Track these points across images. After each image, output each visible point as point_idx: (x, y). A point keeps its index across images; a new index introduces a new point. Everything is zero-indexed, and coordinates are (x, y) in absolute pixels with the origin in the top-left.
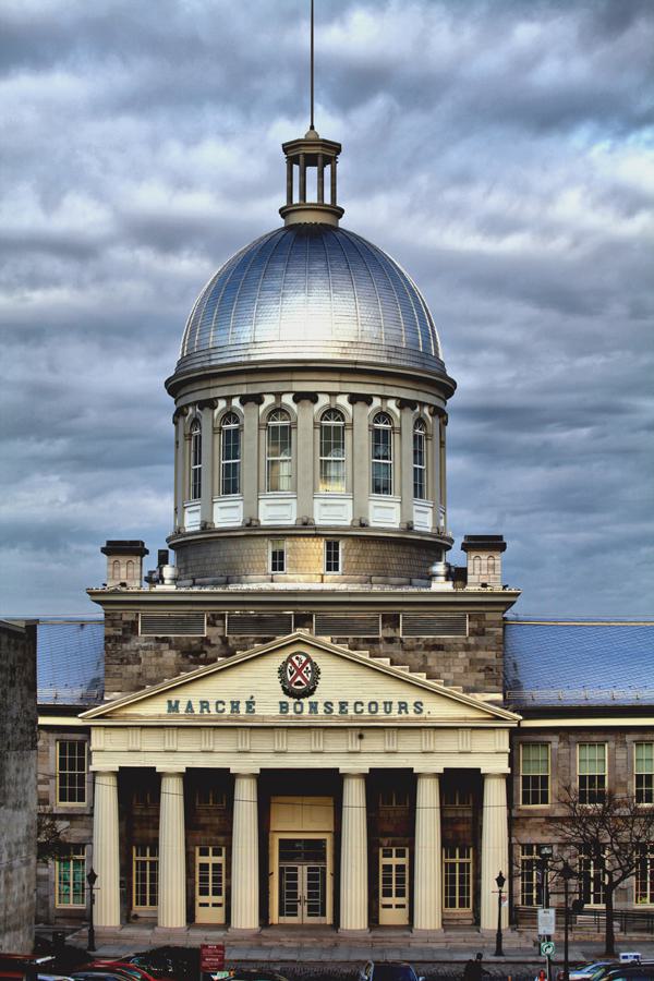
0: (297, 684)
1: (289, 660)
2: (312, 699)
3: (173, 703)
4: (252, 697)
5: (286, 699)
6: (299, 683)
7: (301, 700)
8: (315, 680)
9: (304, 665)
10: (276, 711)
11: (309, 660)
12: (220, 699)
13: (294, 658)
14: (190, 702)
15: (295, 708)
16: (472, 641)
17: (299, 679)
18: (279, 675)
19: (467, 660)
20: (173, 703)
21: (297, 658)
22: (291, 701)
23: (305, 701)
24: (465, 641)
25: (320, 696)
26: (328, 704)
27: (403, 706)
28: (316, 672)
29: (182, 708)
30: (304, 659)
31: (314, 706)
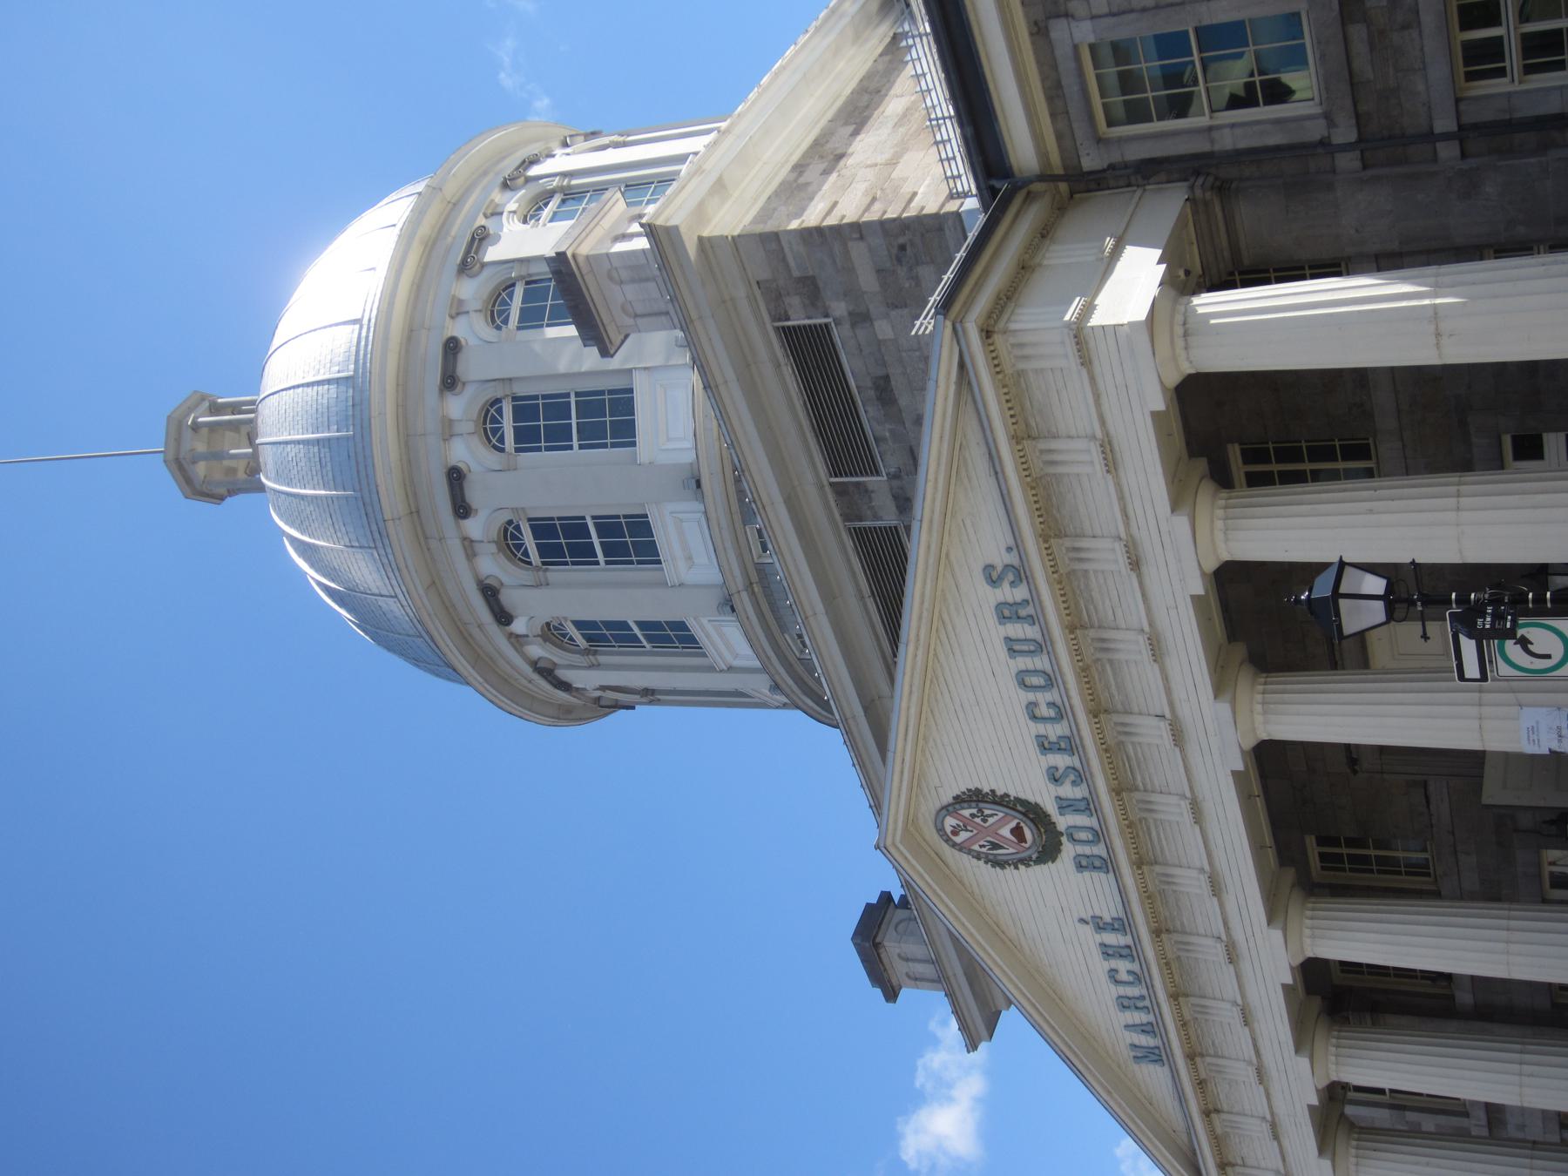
1: (960, 847)
2: (1051, 808)
4: (1082, 921)
6: (1017, 832)
8: (1002, 801)
11: (948, 809)
14: (1127, 1027)
16: (840, 308)
17: (1006, 832)
19: (893, 313)
22: (1068, 850)
23: (1062, 822)
24: (847, 326)
25: (1044, 796)
28: (975, 797)
31: (1065, 805)
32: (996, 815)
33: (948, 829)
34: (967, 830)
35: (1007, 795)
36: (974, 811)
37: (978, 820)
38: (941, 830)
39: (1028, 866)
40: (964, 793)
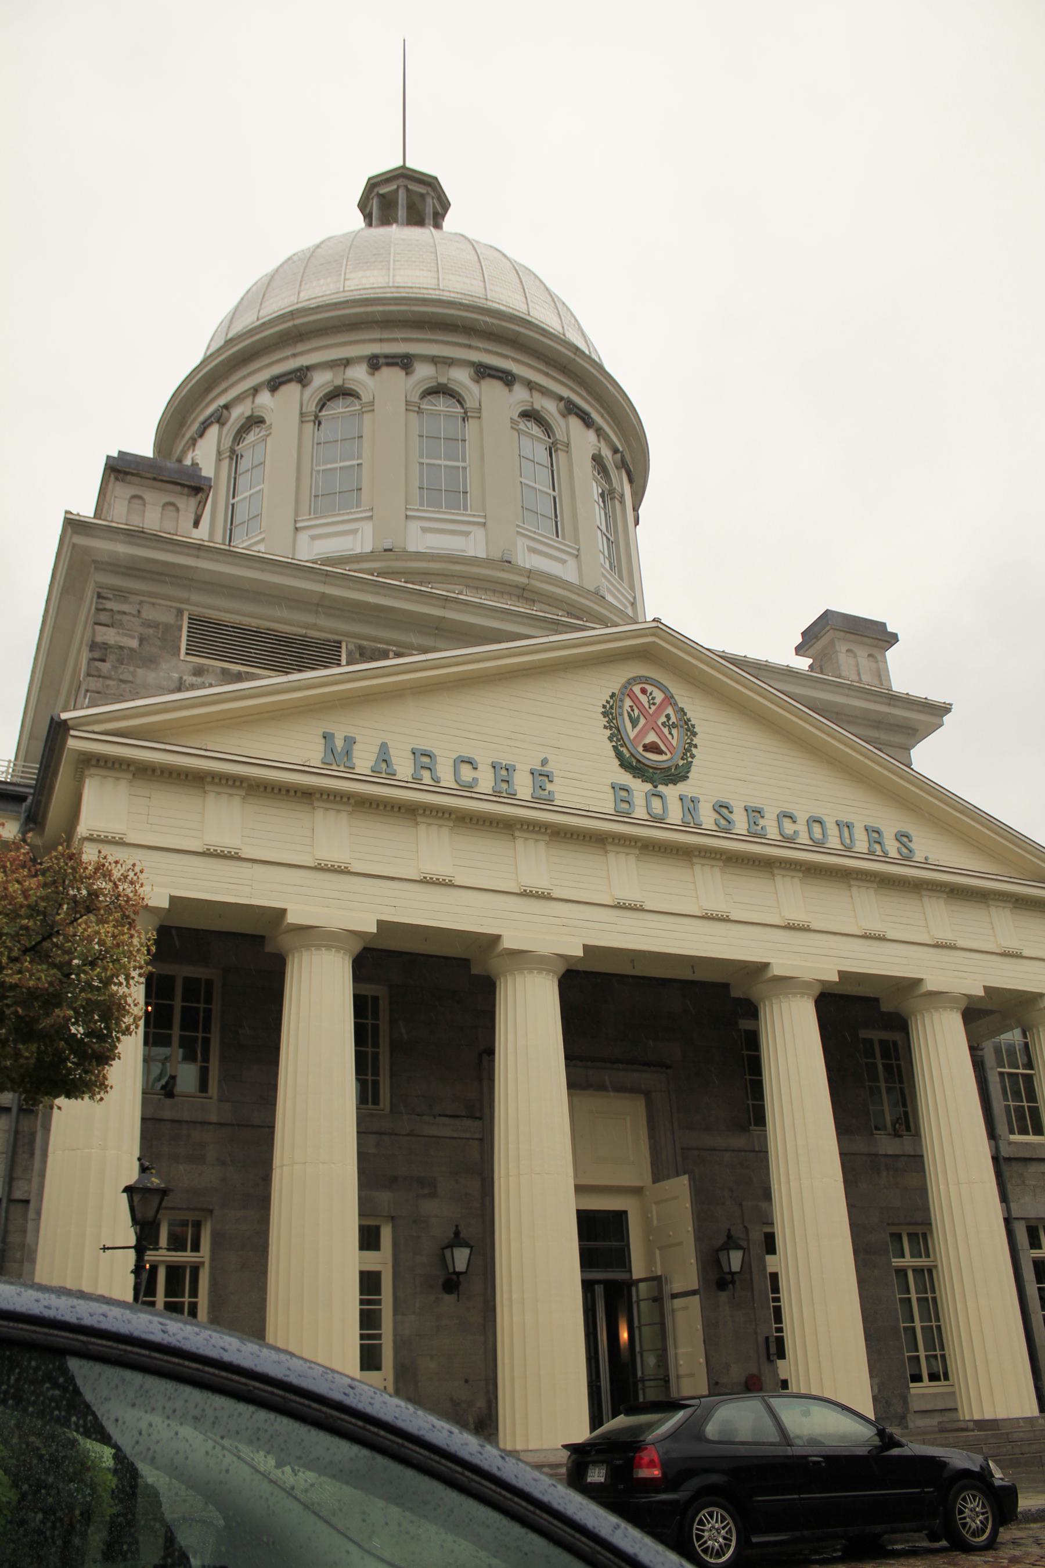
0: (647, 748)
2: (682, 788)
3: (339, 744)
4: (544, 762)
5: (626, 778)
7: (661, 788)
8: (688, 750)
9: (661, 708)
10: (606, 804)
11: (669, 699)
12: (467, 753)
13: (637, 689)
14: (384, 748)
15: (648, 806)
17: (651, 737)
18: (604, 721)
20: (339, 744)
21: (644, 691)
22: (640, 788)
23: (671, 792)
26: (722, 808)
27: (874, 834)
29: (364, 761)
30: (659, 696)
31: (690, 805)
32: (675, 738)
33: (649, 688)
34: (650, 704)
35: (693, 756)
36: (673, 719)
37: (663, 719)
38: (647, 680)
39: (610, 739)
40: (689, 720)
